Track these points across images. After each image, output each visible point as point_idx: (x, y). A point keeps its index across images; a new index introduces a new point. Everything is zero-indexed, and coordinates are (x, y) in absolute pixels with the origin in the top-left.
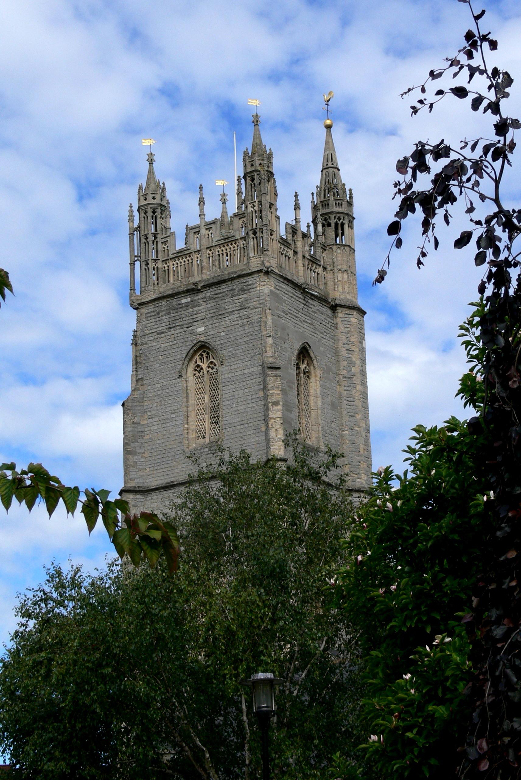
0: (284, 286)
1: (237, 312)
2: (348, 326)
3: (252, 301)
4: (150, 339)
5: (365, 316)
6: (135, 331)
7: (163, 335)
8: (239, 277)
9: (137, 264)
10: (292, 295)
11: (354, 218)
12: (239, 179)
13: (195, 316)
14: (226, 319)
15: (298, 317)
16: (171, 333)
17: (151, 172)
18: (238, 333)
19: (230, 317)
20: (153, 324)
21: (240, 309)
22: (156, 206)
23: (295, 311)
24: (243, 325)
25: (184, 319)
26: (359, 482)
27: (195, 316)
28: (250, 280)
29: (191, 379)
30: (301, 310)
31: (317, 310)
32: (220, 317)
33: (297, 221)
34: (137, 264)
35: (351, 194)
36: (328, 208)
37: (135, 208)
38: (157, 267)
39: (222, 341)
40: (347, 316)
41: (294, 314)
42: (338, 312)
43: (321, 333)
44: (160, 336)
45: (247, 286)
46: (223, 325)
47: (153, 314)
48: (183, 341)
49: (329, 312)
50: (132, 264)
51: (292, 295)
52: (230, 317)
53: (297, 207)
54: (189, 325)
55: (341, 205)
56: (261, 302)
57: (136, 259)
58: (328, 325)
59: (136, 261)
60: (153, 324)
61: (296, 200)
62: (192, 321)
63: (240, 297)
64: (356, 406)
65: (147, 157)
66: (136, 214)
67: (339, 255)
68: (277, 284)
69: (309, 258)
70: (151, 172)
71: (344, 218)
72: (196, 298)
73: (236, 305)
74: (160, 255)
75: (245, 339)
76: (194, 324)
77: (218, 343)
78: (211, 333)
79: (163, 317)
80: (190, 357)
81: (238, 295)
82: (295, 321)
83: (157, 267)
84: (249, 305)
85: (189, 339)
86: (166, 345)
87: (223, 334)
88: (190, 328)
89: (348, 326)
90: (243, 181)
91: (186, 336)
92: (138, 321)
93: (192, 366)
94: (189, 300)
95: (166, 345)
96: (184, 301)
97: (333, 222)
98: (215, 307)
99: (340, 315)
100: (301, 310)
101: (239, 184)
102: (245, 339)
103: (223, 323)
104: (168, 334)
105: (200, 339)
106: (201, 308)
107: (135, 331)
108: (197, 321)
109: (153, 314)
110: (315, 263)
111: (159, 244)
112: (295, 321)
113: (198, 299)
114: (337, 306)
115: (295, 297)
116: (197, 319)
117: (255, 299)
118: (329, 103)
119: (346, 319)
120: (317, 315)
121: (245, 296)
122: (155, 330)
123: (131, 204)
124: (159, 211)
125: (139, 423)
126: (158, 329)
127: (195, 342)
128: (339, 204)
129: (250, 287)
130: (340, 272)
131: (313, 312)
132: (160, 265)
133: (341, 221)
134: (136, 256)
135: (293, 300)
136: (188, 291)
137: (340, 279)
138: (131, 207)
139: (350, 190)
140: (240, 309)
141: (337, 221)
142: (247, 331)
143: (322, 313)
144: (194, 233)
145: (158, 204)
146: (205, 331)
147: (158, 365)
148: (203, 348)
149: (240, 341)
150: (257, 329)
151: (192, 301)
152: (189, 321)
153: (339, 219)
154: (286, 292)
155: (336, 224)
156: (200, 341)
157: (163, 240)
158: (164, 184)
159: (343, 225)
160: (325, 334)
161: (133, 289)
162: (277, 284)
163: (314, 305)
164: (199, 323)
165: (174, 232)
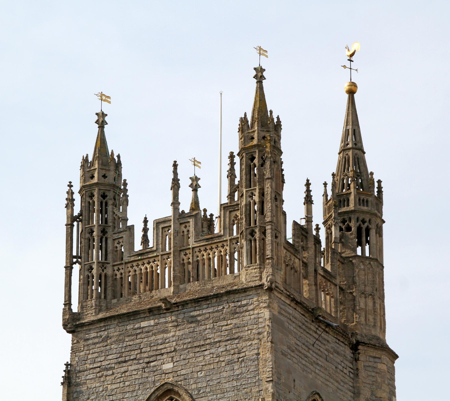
0: (291, 311)
1: (224, 344)
2: (373, 374)
3: (246, 328)
4: (91, 376)
5: (397, 361)
6: (67, 365)
7: (110, 372)
8: (228, 293)
9: (76, 268)
10: (300, 324)
11: (384, 222)
12: (232, 156)
13: (160, 347)
14: (206, 353)
15: (307, 357)
16: (123, 370)
17: (102, 141)
18: (225, 374)
19: (213, 351)
20: (96, 355)
21: (228, 340)
22: (108, 188)
23: (304, 347)
24: (229, 363)
25: (143, 350)
27: (160, 347)
30: (311, 347)
31: (332, 348)
32: (198, 349)
33: (309, 219)
34: (76, 268)
35: (380, 188)
36: (348, 205)
37: (76, 188)
38: (106, 275)
39: (199, 385)
40: (371, 359)
41: (303, 351)
42: (359, 354)
43: (337, 382)
44: (105, 373)
45: (239, 307)
46: (201, 362)
47: (96, 340)
48: (140, 381)
49: (348, 352)
50: (69, 269)
51: (300, 324)
52: (213, 351)
53: (308, 200)
54: (151, 359)
55: (367, 201)
56: (260, 330)
57: (75, 260)
58: (345, 371)
59: (75, 263)
60: (96, 355)
61: (308, 191)
62: (155, 353)
63: (229, 322)
65: (96, 118)
66: (77, 198)
67: (363, 273)
68: (282, 306)
69: (322, 274)
70: (102, 141)
71: (370, 221)
72: (162, 320)
73: (223, 334)
74: (110, 256)
75: (235, 383)
76: (159, 357)
77: (194, 386)
78: (183, 372)
79: (112, 346)
81: (224, 319)
82: (304, 362)
83: (106, 275)
84: (242, 334)
85: (150, 379)
86: (114, 386)
87: (200, 375)
88: (152, 364)
89: (373, 374)
90: (237, 160)
91: (146, 375)
92: (74, 351)
94: (152, 322)
95: (114, 386)
96: (144, 324)
97: (353, 225)
98: (191, 334)
99: (362, 358)
100: (311, 347)
101: (232, 164)
102: (235, 383)
103: (201, 358)
104: (119, 370)
105: (166, 381)
106: (169, 335)
107: (67, 365)
108: (162, 354)
109: (96, 340)
110: (329, 281)
111: (110, 242)
112: (304, 362)
113: (166, 323)
114: (358, 343)
115: (304, 327)
116: (163, 351)
117: (250, 327)
118: (353, 58)
119: (370, 364)
120: (331, 356)
121: (234, 321)
122: (99, 364)
123: (70, 182)
124: (110, 195)
126: (103, 363)
127: (158, 384)
128: (363, 200)
129: (245, 308)
130: (363, 296)
131: (326, 350)
132: (109, 271)
133: (366, 224)
134: (75, 257)
135: (302, 331)
136: (150, 310)
137: (362, 305)
138: (70, 186)
139: (379, 182)
140: (228, 340)
141: (360, 225)
142: (238, 372)
143: (338, 353)
144: (163, 228)
145: (109, 185)
146: (175, 369)
149: (227, 385)
150: (252, 369)
151: (156, 324)
152: (151, 353)
153: (364, 222)
154: (294, 320)
155: (359, 229)
156: (166, 383)
157: (115, 236)
158: (119, 156)
159: (368, 230)
160: (342, 384)
161: (68, 303)
162: (282, 306)
163: (328, 341)
164: (165, 356)
165: (133, 226)
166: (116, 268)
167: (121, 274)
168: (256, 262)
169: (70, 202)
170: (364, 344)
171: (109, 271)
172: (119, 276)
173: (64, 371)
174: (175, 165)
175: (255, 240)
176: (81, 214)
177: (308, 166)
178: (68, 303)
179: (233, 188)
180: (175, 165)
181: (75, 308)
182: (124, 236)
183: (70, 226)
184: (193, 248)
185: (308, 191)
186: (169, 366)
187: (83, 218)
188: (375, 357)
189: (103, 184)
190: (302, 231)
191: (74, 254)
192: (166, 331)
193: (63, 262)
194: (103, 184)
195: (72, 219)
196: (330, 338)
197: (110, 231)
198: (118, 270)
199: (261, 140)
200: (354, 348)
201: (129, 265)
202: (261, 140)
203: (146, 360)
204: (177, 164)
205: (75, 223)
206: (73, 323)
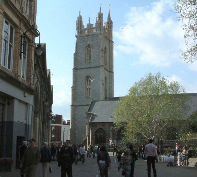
29: (86, 51)
49: (109, 42)
80: (86, 47)
93: (86, 49)
148: (89, 46)
169: (76, 22)
177: (105, 19)
179: (97, 21)
181: (77, 35)
183: (76, 25)
186: (89, 43)
189: (80, 20)
190: (104, 27)
194: (80, 20)
195: (76, 24)
196: (107, 40)
199: (100, 16)
200: (109, 41)
202: (100, 16)
204: (90, 19)
206: (77, 37)
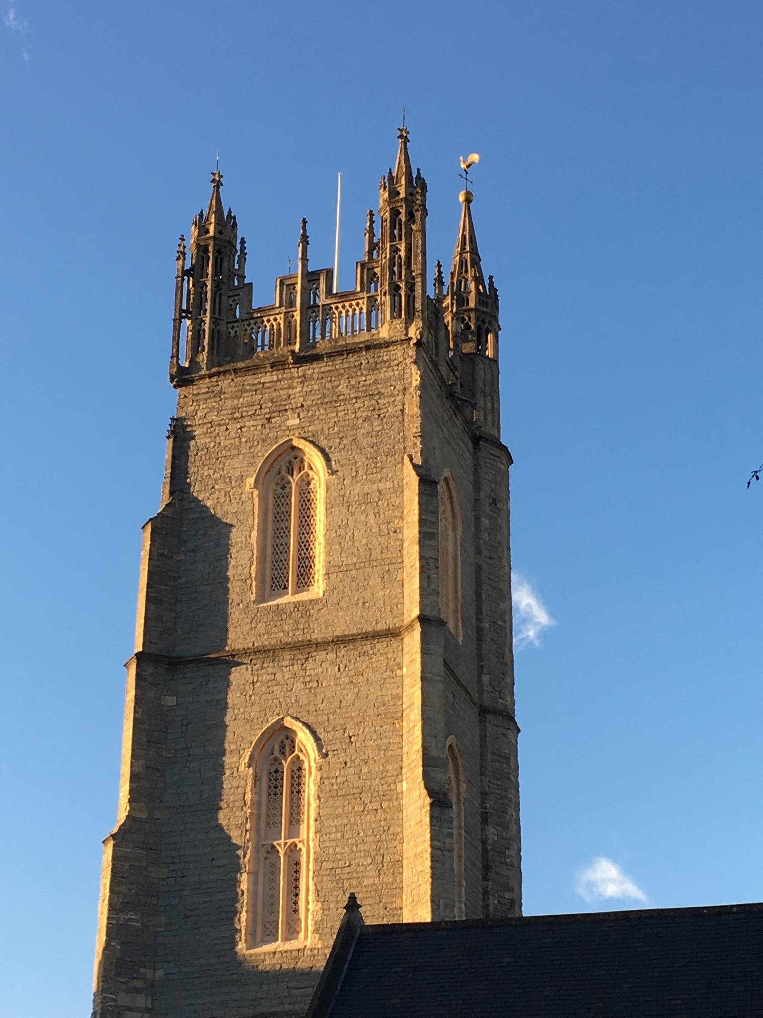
26: (502, 704)
28: (384, 355)
40: (492, 457)
50: (178, 322)
64: (501, 590)
78: (310, 429)
107: (173, 419)
111: (224, 298)
114: (480, 438)
125: (172, 557)
132: (223, 328)
133: (486, 325)
134: (184, 311)
145: (225, 241)
147: (211, 472)
157: (231, 293)
161: (176, 356)
165: (251, 284)
166: (230, 326)
167: (236, 332)
168: (400, 316)
170: (486, 440)
171: (223, 328)
172: (233, 334)
173: (170, 425)
174: (304, 222)
175: (400, 296)
176: (192, 269)
178: (176, 356)
180: (304, 222)
182: (241, 293)
184: (323, 305)
185: (440, 273)
186: (294, 422)
187: (195, 272)
188: (494, 455)
191: (184, 307)
192: (290, 387)
193: (172, 314)
197: (225, 287)
198: (233, 328)
201: (246, 323)
203: (267, 416)
205: (186, 278)
